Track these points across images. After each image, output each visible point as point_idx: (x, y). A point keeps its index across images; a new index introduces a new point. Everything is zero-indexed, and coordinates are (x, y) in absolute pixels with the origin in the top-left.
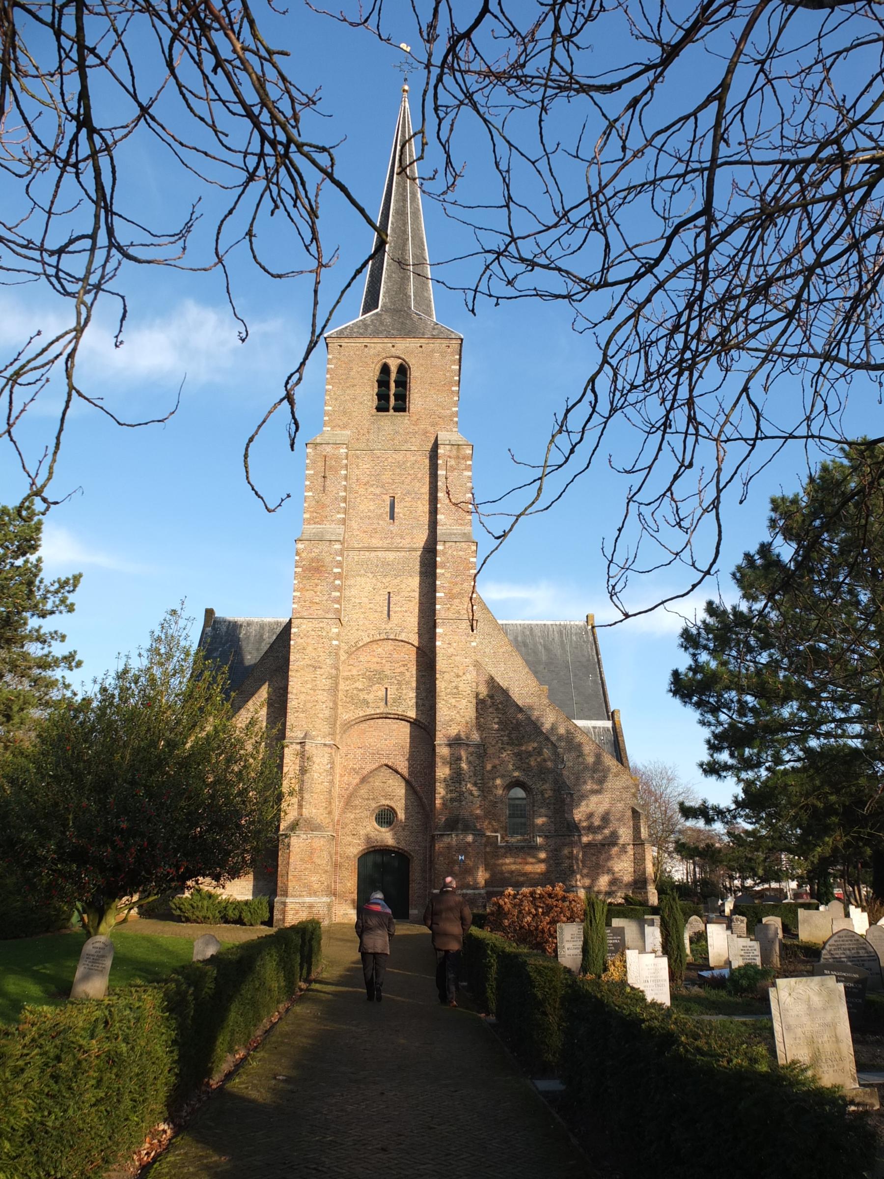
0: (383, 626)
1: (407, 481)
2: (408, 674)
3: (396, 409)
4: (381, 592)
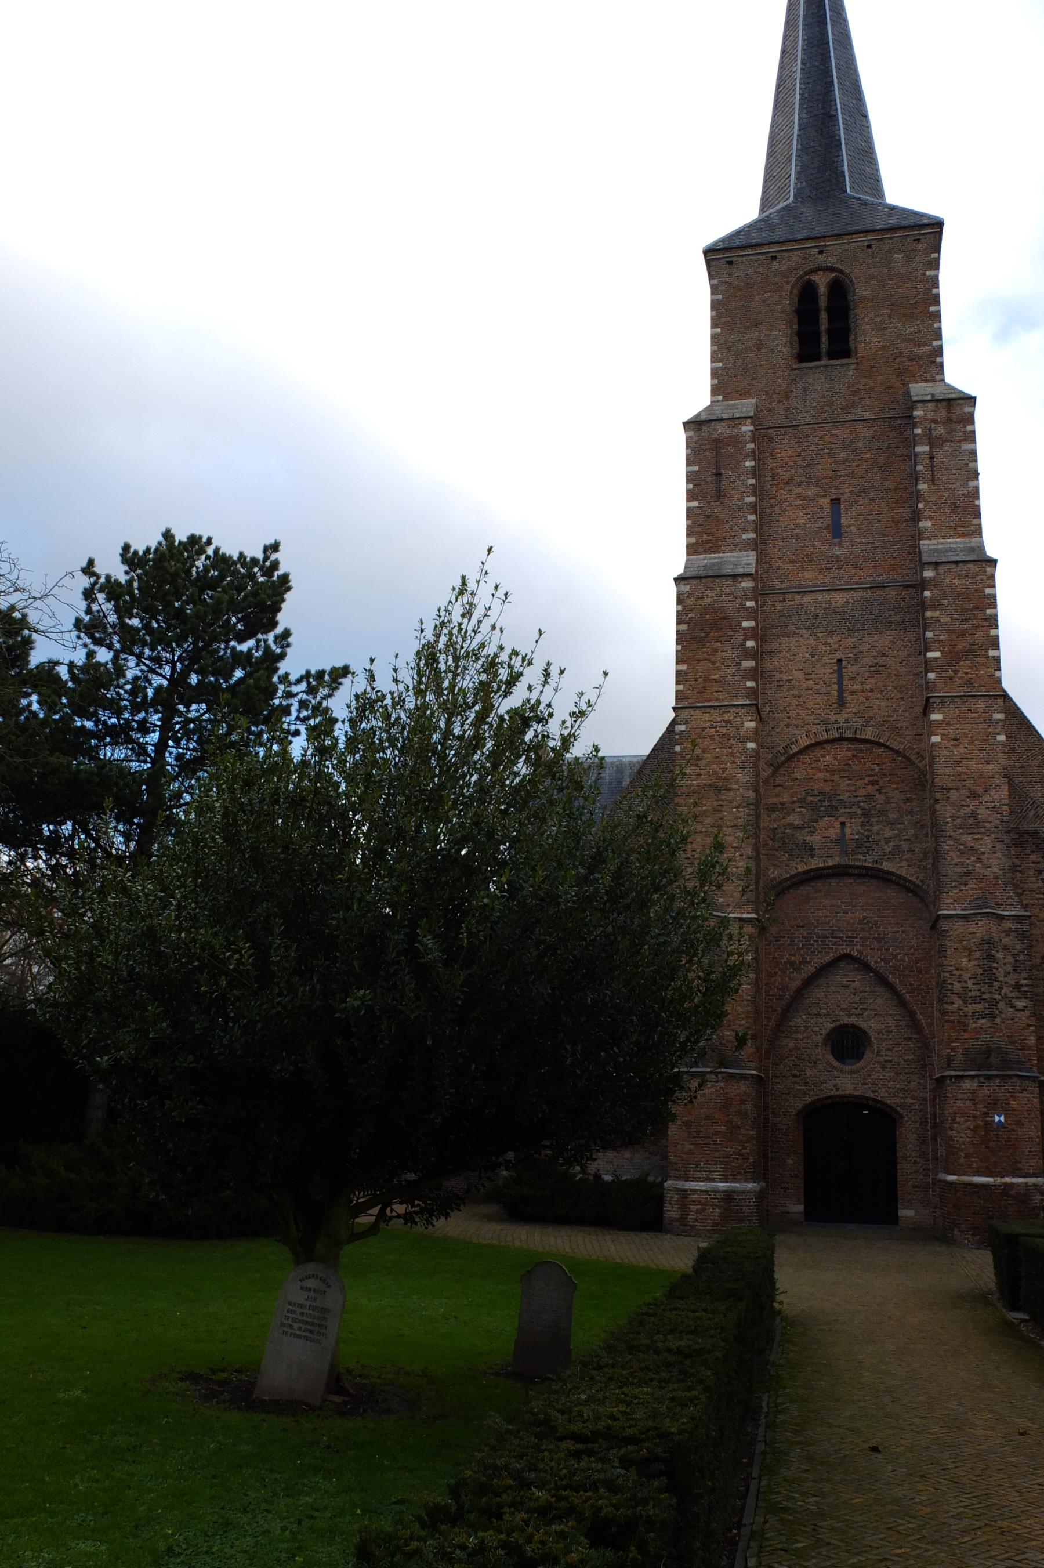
0: (833, 717)
1: (860, 471)
3: (831, 356)
4: (825, 660)
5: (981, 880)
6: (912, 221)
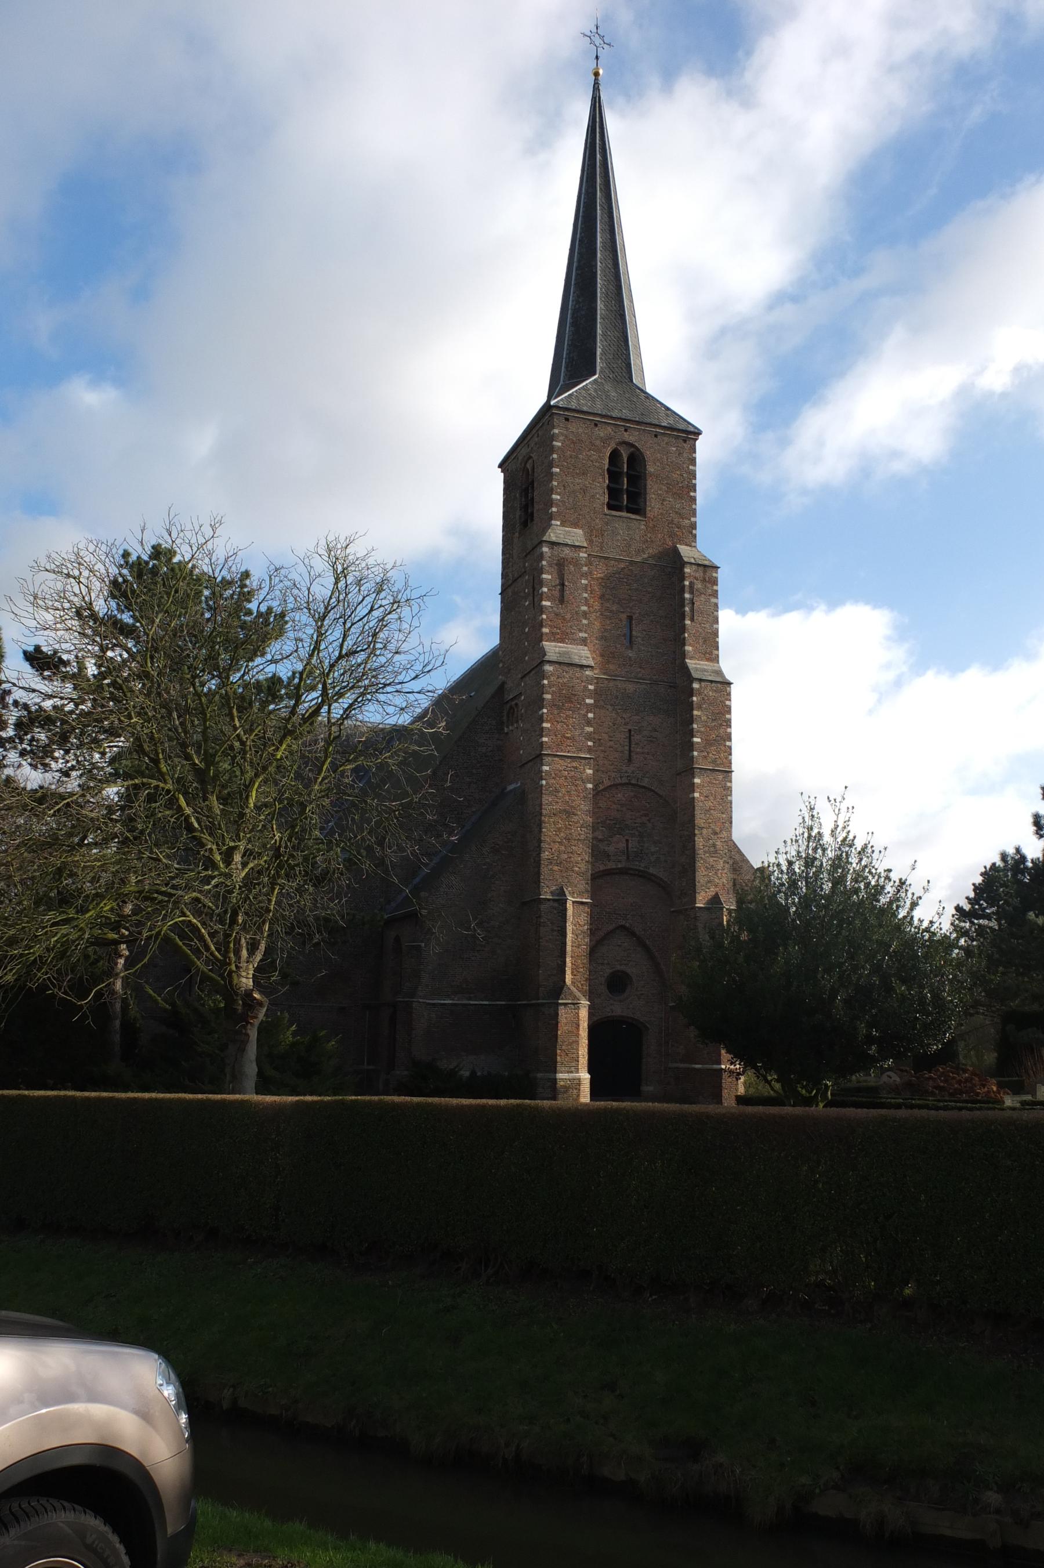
2: (649, 825)
5: (716, 886)
6: (682, 426)
